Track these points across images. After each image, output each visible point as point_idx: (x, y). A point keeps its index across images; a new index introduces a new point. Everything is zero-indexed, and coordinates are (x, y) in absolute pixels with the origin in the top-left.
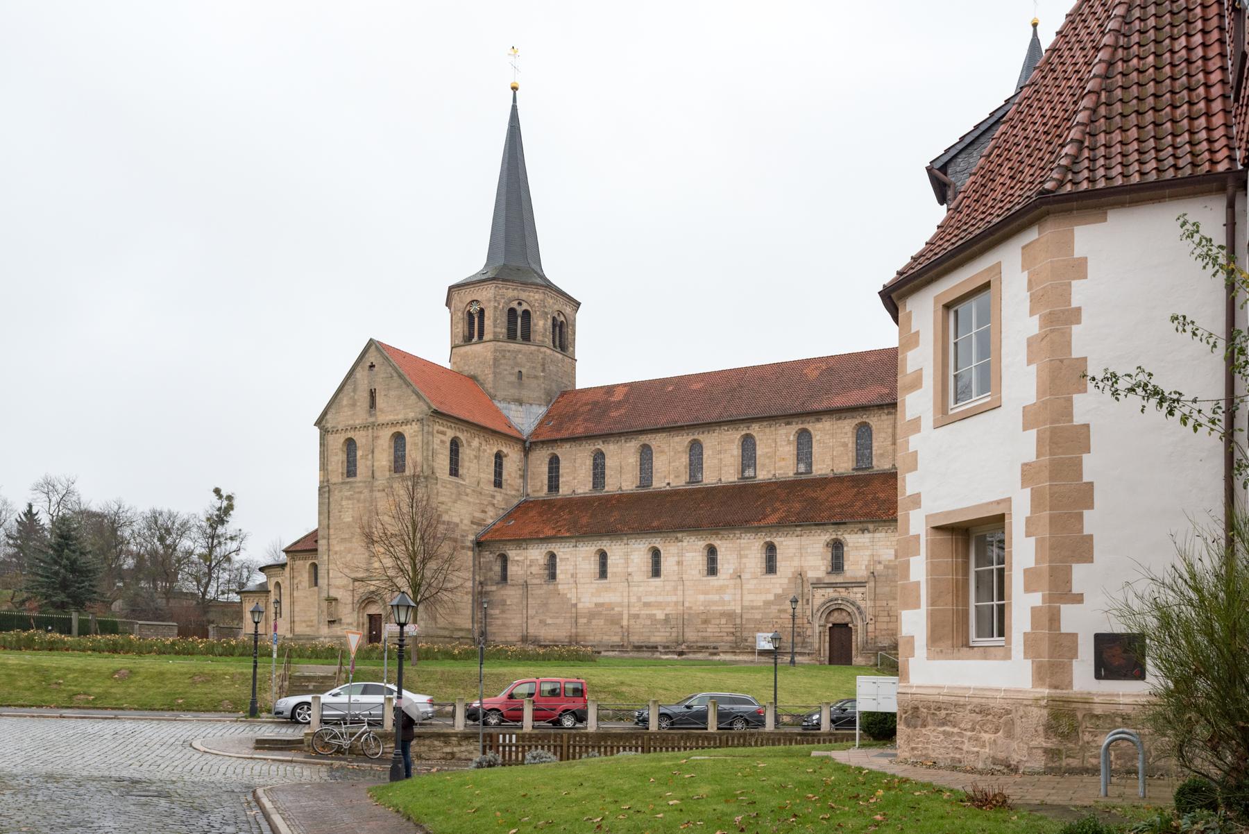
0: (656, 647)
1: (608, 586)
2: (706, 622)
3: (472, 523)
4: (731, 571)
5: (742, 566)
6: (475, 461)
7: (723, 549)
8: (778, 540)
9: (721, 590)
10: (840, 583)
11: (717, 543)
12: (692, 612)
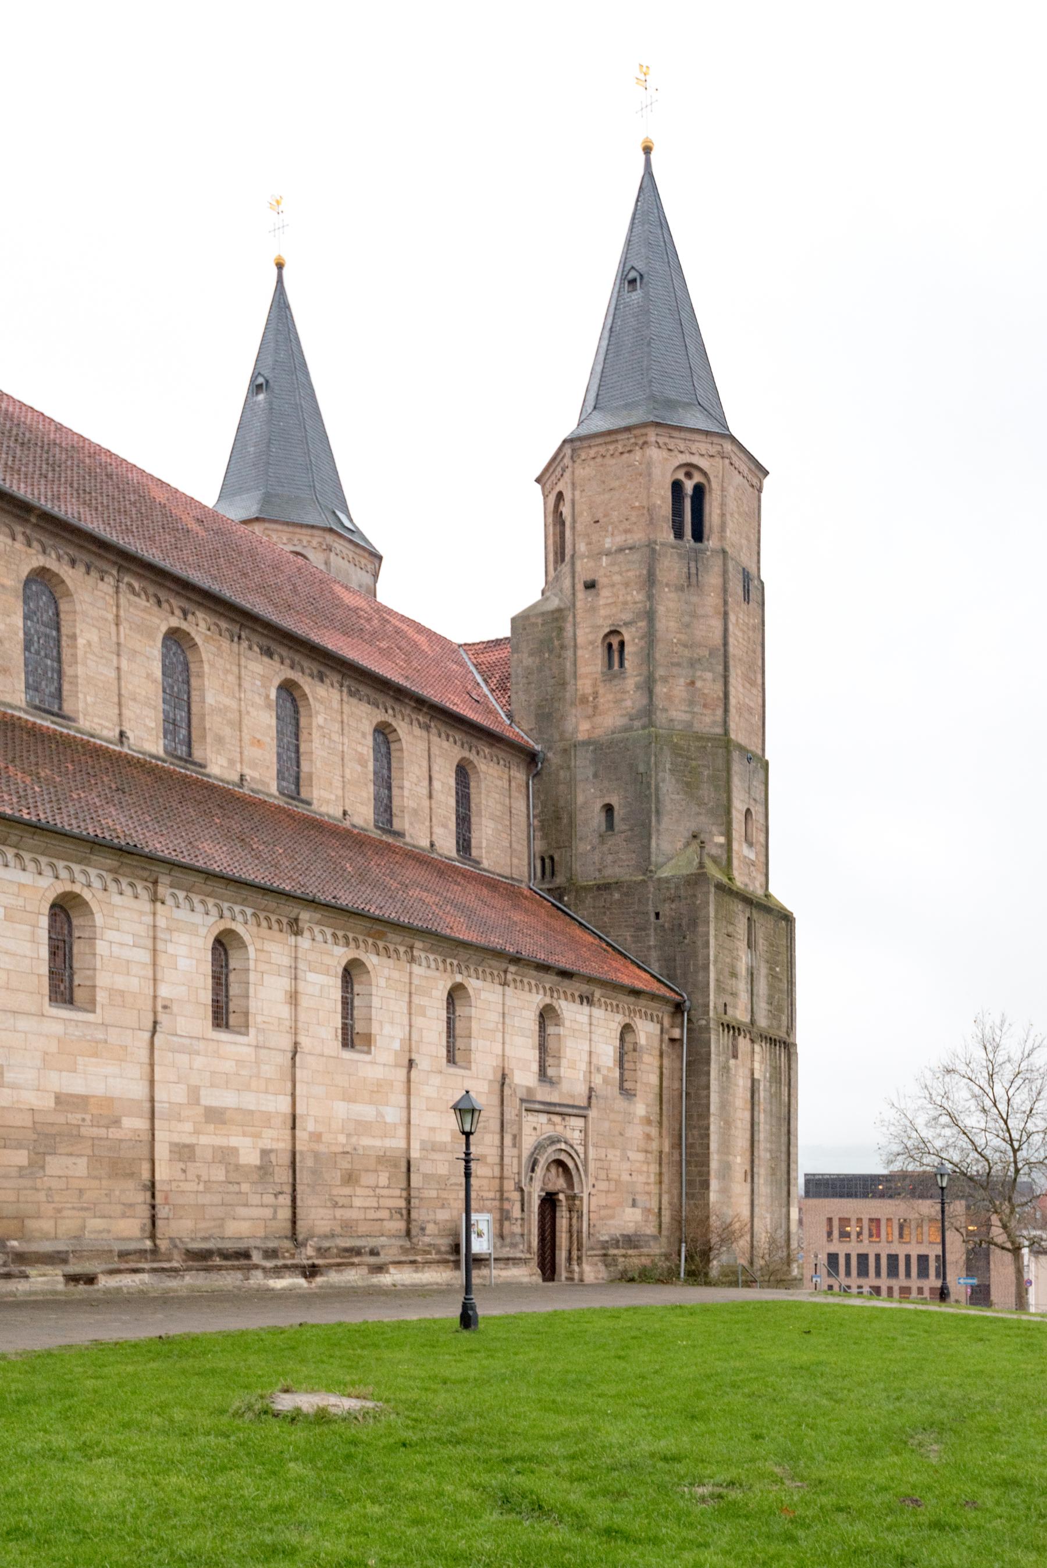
0: (246, 1255)
1: (100, 1036)
2: (350, 1178)
4: (396, 1045)
5: (415, 1037)
7: (382, 982)
8: (473, 984)
9: (377, 1091)
10: (560, 1105)
11: (372, 960)
12: (322, 1148)
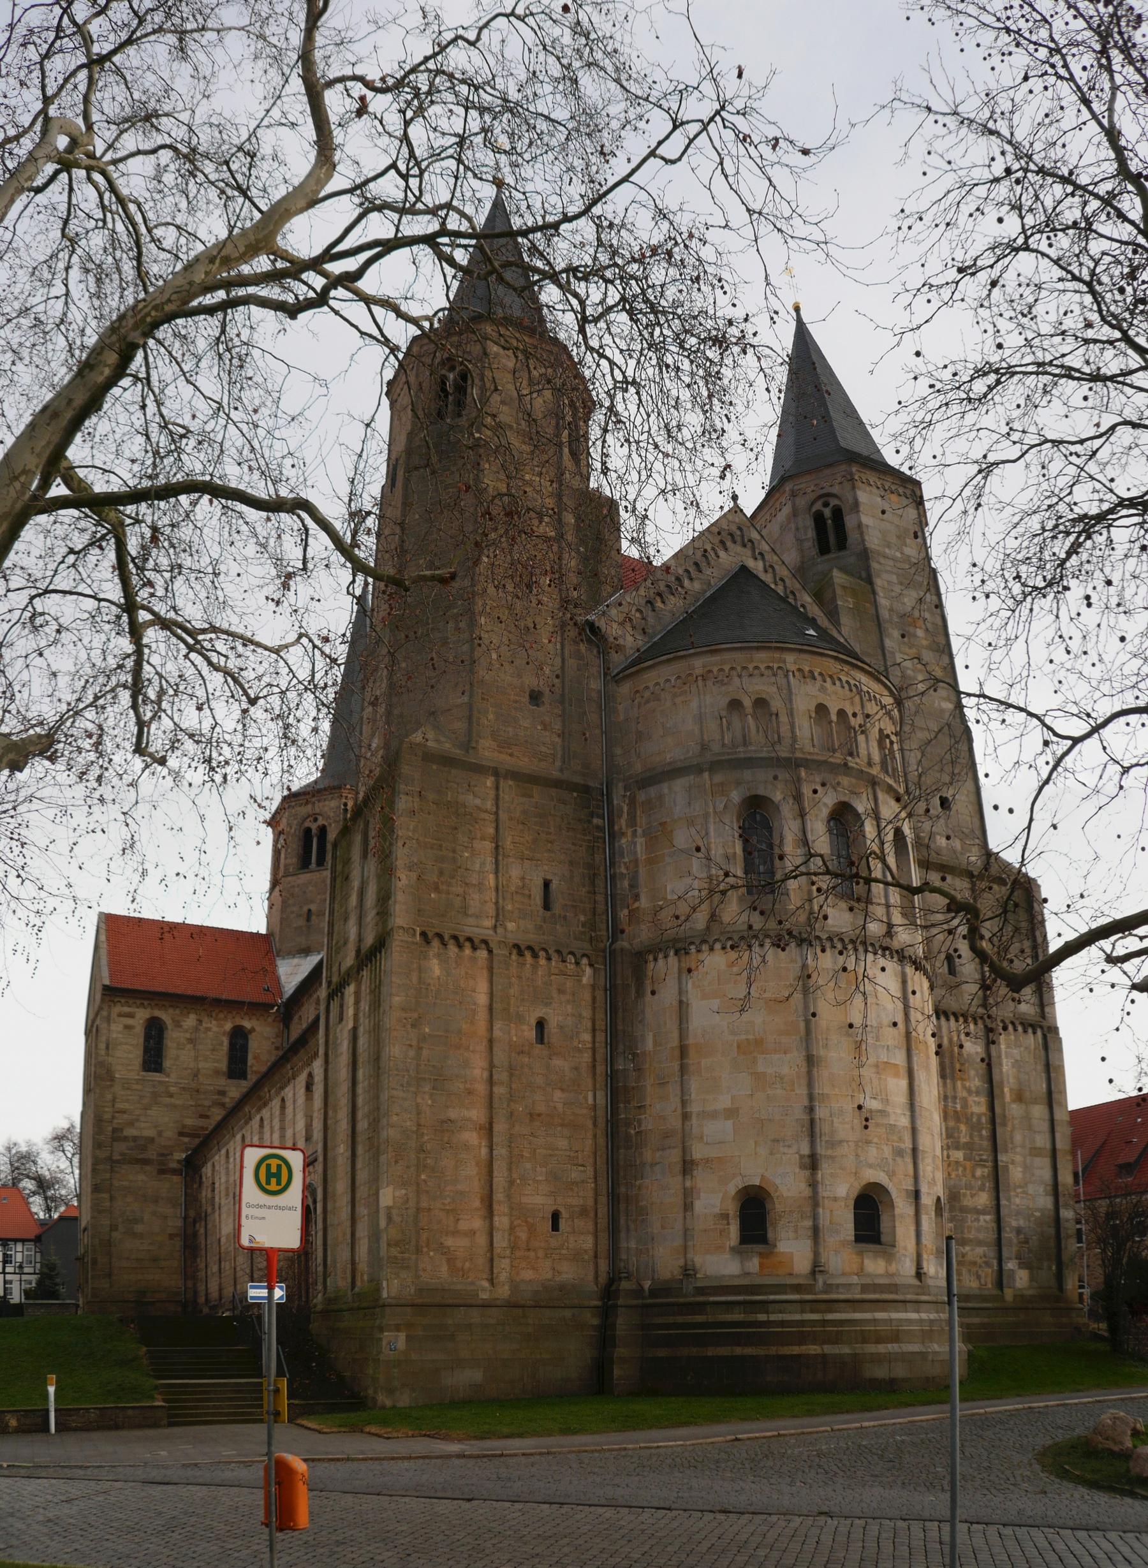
3: (181, 1134)
6: (190, 1046)
